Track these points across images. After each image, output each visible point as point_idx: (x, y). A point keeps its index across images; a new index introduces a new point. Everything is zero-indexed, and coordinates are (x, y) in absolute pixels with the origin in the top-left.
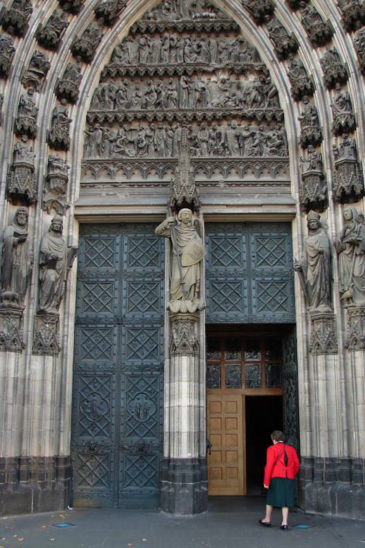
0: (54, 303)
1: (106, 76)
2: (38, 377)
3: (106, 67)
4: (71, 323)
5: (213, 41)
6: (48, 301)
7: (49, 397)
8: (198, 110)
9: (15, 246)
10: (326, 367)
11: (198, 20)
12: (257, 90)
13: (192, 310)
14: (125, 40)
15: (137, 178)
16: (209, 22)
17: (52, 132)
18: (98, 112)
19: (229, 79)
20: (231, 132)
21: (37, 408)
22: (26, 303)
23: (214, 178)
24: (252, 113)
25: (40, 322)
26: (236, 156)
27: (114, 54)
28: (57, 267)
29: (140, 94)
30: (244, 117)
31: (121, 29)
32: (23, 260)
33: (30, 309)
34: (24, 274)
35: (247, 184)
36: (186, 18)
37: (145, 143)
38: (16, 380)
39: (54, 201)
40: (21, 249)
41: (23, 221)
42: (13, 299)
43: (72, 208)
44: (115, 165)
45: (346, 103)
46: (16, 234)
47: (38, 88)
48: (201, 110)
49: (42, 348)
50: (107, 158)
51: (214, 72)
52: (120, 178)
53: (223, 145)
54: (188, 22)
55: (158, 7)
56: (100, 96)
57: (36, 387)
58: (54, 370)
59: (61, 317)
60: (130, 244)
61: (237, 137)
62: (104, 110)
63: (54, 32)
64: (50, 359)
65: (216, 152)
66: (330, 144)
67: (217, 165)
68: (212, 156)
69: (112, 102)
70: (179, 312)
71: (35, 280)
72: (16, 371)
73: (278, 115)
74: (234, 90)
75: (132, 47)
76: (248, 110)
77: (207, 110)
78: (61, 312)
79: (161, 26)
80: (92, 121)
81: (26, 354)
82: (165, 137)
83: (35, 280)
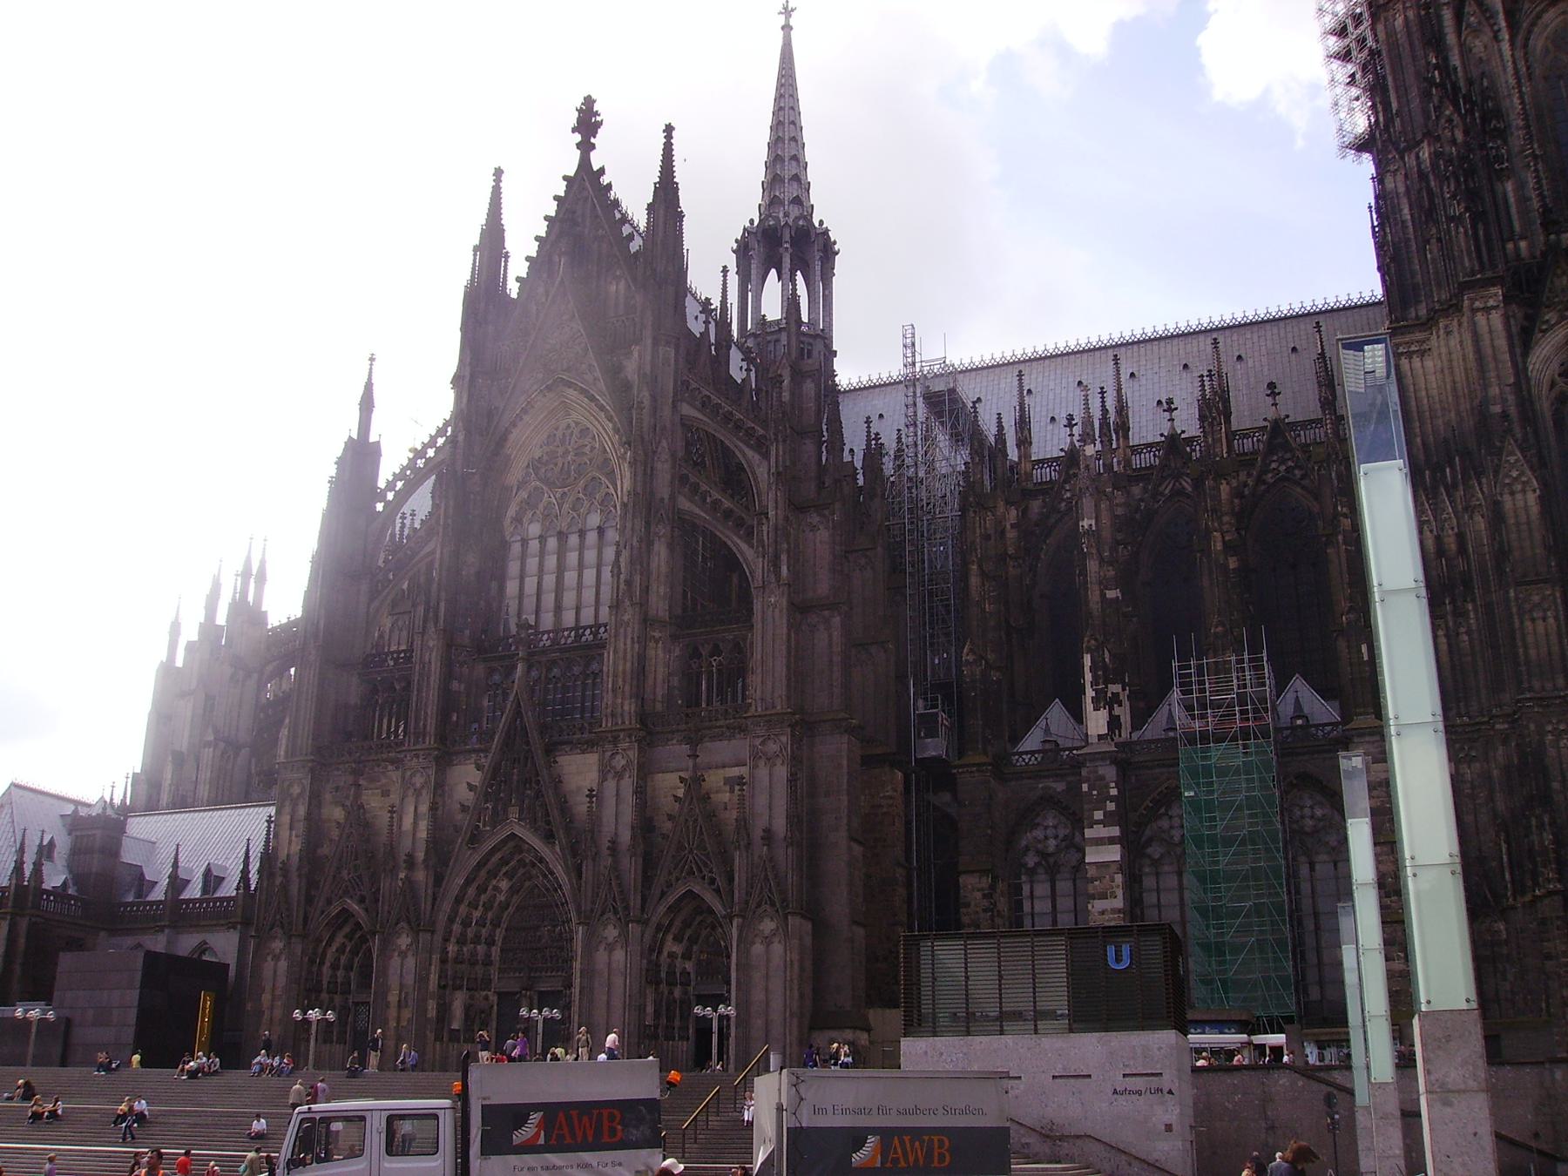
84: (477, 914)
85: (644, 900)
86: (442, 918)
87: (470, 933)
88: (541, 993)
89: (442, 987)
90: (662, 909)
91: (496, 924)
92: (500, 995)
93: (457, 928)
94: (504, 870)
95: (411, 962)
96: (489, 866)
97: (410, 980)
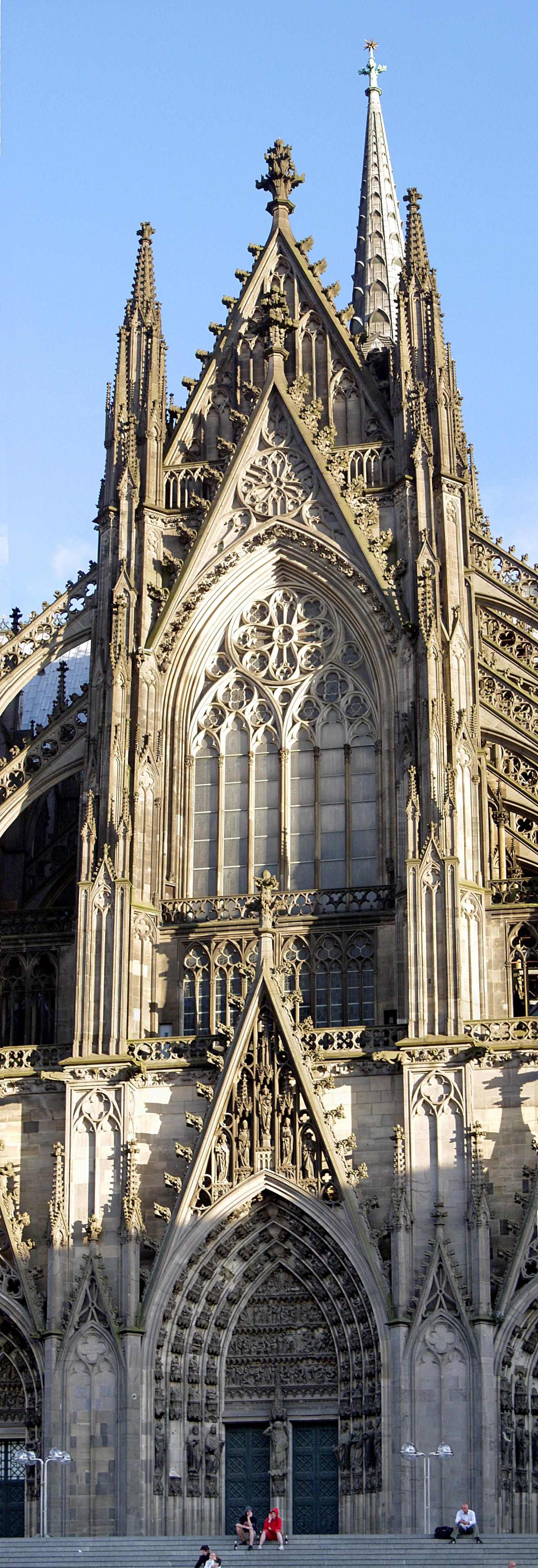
1: (236, 1332)
2: (208, 1508)
4: (223, 1480)
6: (211, 1471)
7: (213, 1518)
13: (281, 1474)
15: (255, 1398)
17: (207, 1377)
20: (307, 1368)
21: (208, 1523)
26: (309, 1384)
27: (240, 1318)
30: (314, 1359)
31: (243, 1303)
33: (202, 1475)
34: (199, 1459)
35: (315, 1401)
36: (282, 1292)
40: (197, 1447)
42: (195, 1472)
45: (359, 1363)
51: (299, 1328)
52: (246, 1398)
55: (266, 1282)
56: (232, 1346)
57: (207, 1514)
61: (310, 1372)
64: (213, 1499)
65: (298, 1382)
66: (354, 1384)
67: (299, 1389)
68: (297, 1385)
71: (204, 1461)
75: (249, 1310)
76: (316, 1354)
78: (217, 1475)
80: (229, 1363)
83: (204, 1461)
84: (197, 1310)
85: (494, 1294)
86: (153, 1313)
87: (188, 1336)
88: (296, 1424)
89: (158, 1417)
90: (522, 1303)
91: (221, 1327)
92: (229, 1426)
93: (171, 1328)
94: (240, 1245)
95: (105, 1378)
96: (221, 1238)
97: (108, 1405)
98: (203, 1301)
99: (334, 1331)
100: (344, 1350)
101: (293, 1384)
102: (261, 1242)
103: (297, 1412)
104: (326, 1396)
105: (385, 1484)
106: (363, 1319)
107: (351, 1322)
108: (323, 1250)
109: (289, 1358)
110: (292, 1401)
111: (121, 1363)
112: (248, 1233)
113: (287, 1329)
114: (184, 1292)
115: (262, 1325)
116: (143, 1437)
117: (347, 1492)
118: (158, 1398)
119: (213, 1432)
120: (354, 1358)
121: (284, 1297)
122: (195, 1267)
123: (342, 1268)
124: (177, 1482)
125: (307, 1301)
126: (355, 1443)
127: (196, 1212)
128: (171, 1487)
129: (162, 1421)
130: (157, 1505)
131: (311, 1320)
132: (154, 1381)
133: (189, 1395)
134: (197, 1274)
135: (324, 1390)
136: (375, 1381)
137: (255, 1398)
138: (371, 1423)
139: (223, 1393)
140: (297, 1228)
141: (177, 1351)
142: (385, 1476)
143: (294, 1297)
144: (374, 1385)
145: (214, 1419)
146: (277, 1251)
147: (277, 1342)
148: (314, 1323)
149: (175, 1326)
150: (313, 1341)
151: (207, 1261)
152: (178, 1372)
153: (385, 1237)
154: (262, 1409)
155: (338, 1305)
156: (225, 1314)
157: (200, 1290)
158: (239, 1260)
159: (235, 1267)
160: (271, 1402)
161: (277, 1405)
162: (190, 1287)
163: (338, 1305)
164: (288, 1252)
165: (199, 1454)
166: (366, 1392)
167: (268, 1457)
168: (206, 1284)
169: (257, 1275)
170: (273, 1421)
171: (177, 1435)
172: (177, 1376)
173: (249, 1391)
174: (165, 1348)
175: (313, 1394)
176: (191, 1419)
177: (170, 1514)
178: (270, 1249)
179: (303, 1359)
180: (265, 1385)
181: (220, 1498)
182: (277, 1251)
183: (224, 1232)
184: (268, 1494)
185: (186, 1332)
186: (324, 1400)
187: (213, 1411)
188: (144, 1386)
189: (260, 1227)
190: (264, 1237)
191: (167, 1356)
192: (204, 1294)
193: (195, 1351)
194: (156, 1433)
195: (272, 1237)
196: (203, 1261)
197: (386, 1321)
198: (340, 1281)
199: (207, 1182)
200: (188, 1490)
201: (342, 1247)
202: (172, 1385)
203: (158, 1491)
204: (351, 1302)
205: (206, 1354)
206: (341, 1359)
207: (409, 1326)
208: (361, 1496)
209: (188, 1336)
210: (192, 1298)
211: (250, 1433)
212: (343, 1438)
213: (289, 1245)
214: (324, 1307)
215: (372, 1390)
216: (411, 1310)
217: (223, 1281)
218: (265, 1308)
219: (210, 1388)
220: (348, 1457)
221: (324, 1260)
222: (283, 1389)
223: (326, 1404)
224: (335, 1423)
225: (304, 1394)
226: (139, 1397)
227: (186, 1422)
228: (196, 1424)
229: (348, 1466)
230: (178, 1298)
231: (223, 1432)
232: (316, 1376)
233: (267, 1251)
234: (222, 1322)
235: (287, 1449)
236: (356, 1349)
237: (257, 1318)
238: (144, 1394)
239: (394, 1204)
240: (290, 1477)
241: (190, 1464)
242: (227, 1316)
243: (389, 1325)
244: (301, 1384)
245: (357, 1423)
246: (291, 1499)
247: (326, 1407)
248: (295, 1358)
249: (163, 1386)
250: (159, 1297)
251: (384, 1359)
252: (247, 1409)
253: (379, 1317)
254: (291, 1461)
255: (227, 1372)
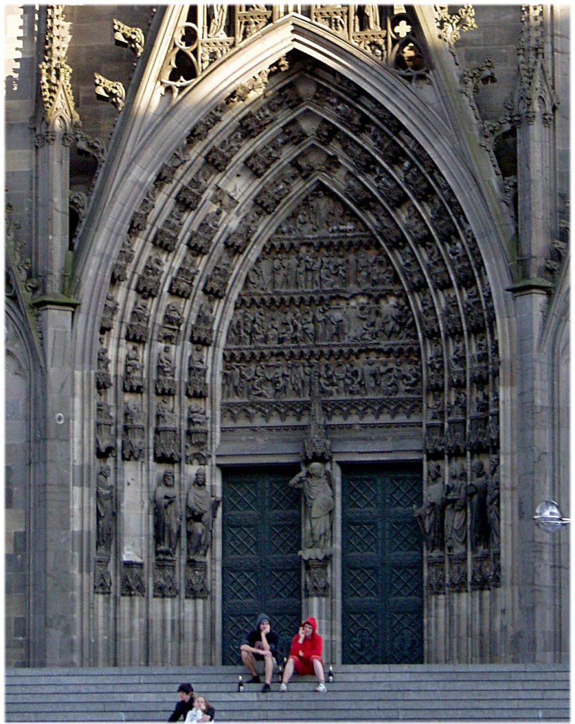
0: (202, 552)
1: (240, 304)
2: (191, 617)
3: (240, 295)
4: (218, 568)
5: (351, 257)
6: (197, 551)
7: (201, 635)
8: (335, 345)
9: (166, 507)
10: (437, 606)
11: (335, 235)
12: (394, 319)
13: (321, 557)
14: (258, 260)
15: (275, 421)
16: (347, 237)
17: (190, 383)
18: (235, 349)
19: (368, 304)
21: (191, 644)
22: (177, 555)
23: (351, 420)
24: (387, 348)
25: (190, 570)
26: (371, 396)
27: (247, 278)
28: (203, 520)
29: (277, 325)
30: (379, 351)
31: (254, 252)
32: (173, 518)
33: (180, 558)
34: (175, 529)
36: (323, 232)
37: (282, 384)
38: (173, 622)
39: (195, 454)
40: (171, 509)
41: (170, 482)
42: (167, 553)
43: (214, 458)
44: (253, 407)
45: (461, 360)
46: (166, 497)
47: (174, 341)
48: (338, 346)
49: (193, 593)
50: (246, 400)
51: (354, 296)
52: (259, 422)
53: (360, 383)
54: (325, 238)
55: (294, 216)
56: (234, 329)
57: (189, 628)
58: (204, 611)
59: (208, 564)
60: (272, 488)
61: (374, 375)
62: (240, 346)
63: (185, 284)
64: (200, 602)
65: (351, 392)
66: (451, 397)
69: (248, 337)
70: (310, 559)
71: (184, 533)
72: (173, 615)
73: (415, 348)
74: (373, 318)
75: (265, 266)
76: (384, 343)
77: (343, 345)
78: (208, 559)
79: (296, 243)
80: (229, 358)
81: (180, 599)
82: (302, 375)
83: (184, 533)
84: (171, 264)
86: (93, 270)
87: (156, 310)
88: (347, 467)
89: (102, 455)
91: (213, 294)
92: (229, 473)
93: (125, 297)
94: (247, 148)
96: (215, 136)
98: (183, 248)
99: (416, 302)
100: (432, 335)
101: (343, 397)
102: (285, 143)
103: (349, 447)
104: (401, 418)
105: (506, 574)
106: (467, 281)
107: (446, 285)
108: (396, 157)
109: (335, 350)
110: (341, 427)
111: (35, 357)
112: (262, 127)
113: (332, 298)
114: (149, 232)
115: (286, 291)
116: (76, 491)
117: (438, 589)
118: (102, 421)
119: (199, 482)
120: (451, 349)
121: (326, 242)
122: (168, 188)
123: (430, 190)
124: (136, 571)
125: (367, 248)
126: (453, 501)
127: (169, 89)
128: (125, 579)
129: (110, 462)
130: (101, 612)
131: (375, 283)
132: (94, 391)
133: (158, 416)
134: (172, 201)
135: (399, 406)
136: (488, 390)
137: (275, 421)
138: (482, 465)
139: (218, 413)
140: (349, 119)
141: (136, 338)
142: (506, 560)
143: (345, 241)
144: (486, 397)
145: (201, 459)
146: (315, 159)
147: (314, 321)
148: (380, 287)
149: (133, 294)
150: (379, 320)
151: (188, 178)
152: (137, 374)
153: (506, 135)
154: (289, 441)
155: (423, 256)
156: (221, 272)
157: (176, 229)
158: (246, 175)
159: (240, 187)
160: (303, 428)
161: (315, 434)
162: (159, 224)
163: (423, 256)
164: (333, 162)
165: (175, 520)
166: (473, 411)
167: (297, 526)
168: (188, 217)
169: (278, 202)
170: (307, 462)
171: (136, 486)
172: (136, 383)
173: (265, 409)
174: (114, 332)
175: (378, 414)
176: (160, 459)
177: (124, 628)
178: (302, 155)
179: (361, 351)
180: (292, 398)
181: (213, 599)
182: (315, 159)
183: (220, 126)
184: (297, 592)
185: (152, 304)
186: (398, 425)
187: (200, 444)
188: (77, 400)
189: (284, 117)
190: (291, 135)
191: (118, 346)
192: (184, 235)
193: (168, 338)
194: (99, 483)
195: (305, 135)
196: (183, 177)
197: (508, 285)
198: (426, 212)
199: (190, 36)
200: (155, 585)
201: (430, 152)
202: (128, 398)
203: (102, 586)
204: (445, 250)
205: (188, 343)
206: (429, 353)
207: (549, 292)
208: (464, 595)
209: (156, 310)
210: (163, 244)
211: (265, 483)
212: (432, 492)
213: (335, 148)
214: (397, 259)
215: (484, 407)
216: (553, 264)
217: (219, 213)
218: (294, 261)
219: (194, 403)
220: (440, 526)
221: (398, 175)
222: (324, 405)
223: (401, 431)
224: (417, 465)
225: (363, 414)
226: (67, 420)
227: (152, 464)
228: (169, 468)
229: (440, 543)
230: (138, 243)
231: (218, 482)
232: (384, 383)
233: (296, 159)
234: (215, 285)
235: (331, 513)
236: (455, 334)
237: (279, 279)
238: (78, 415)
239: (523, 77)
240: (338, 561)
241: (158, 539)
242: (226, 274)
243: (514, 290)
244: (357, 397)
245: (456, 465)
246: (338, 601)
247: (402, 438)
248: (345, 350)
249: (110, 400)
250: (104, 241)
251: (505, 352)
252: (260, 441)
253: (496, 276)
254: (338, 534)
255: (225, 376)
